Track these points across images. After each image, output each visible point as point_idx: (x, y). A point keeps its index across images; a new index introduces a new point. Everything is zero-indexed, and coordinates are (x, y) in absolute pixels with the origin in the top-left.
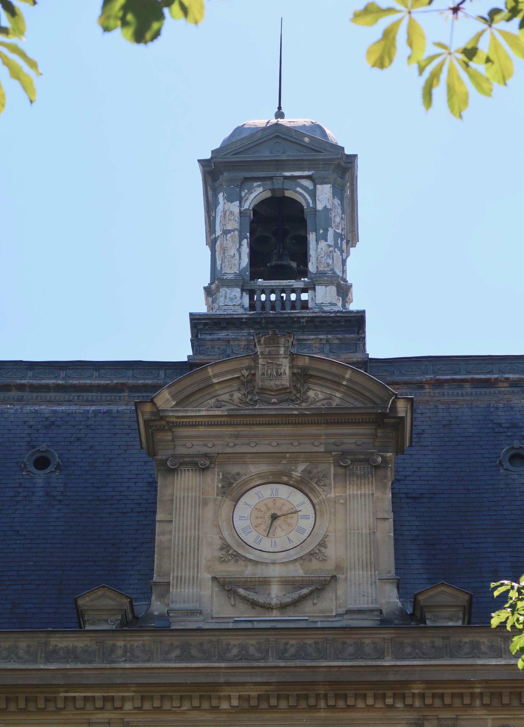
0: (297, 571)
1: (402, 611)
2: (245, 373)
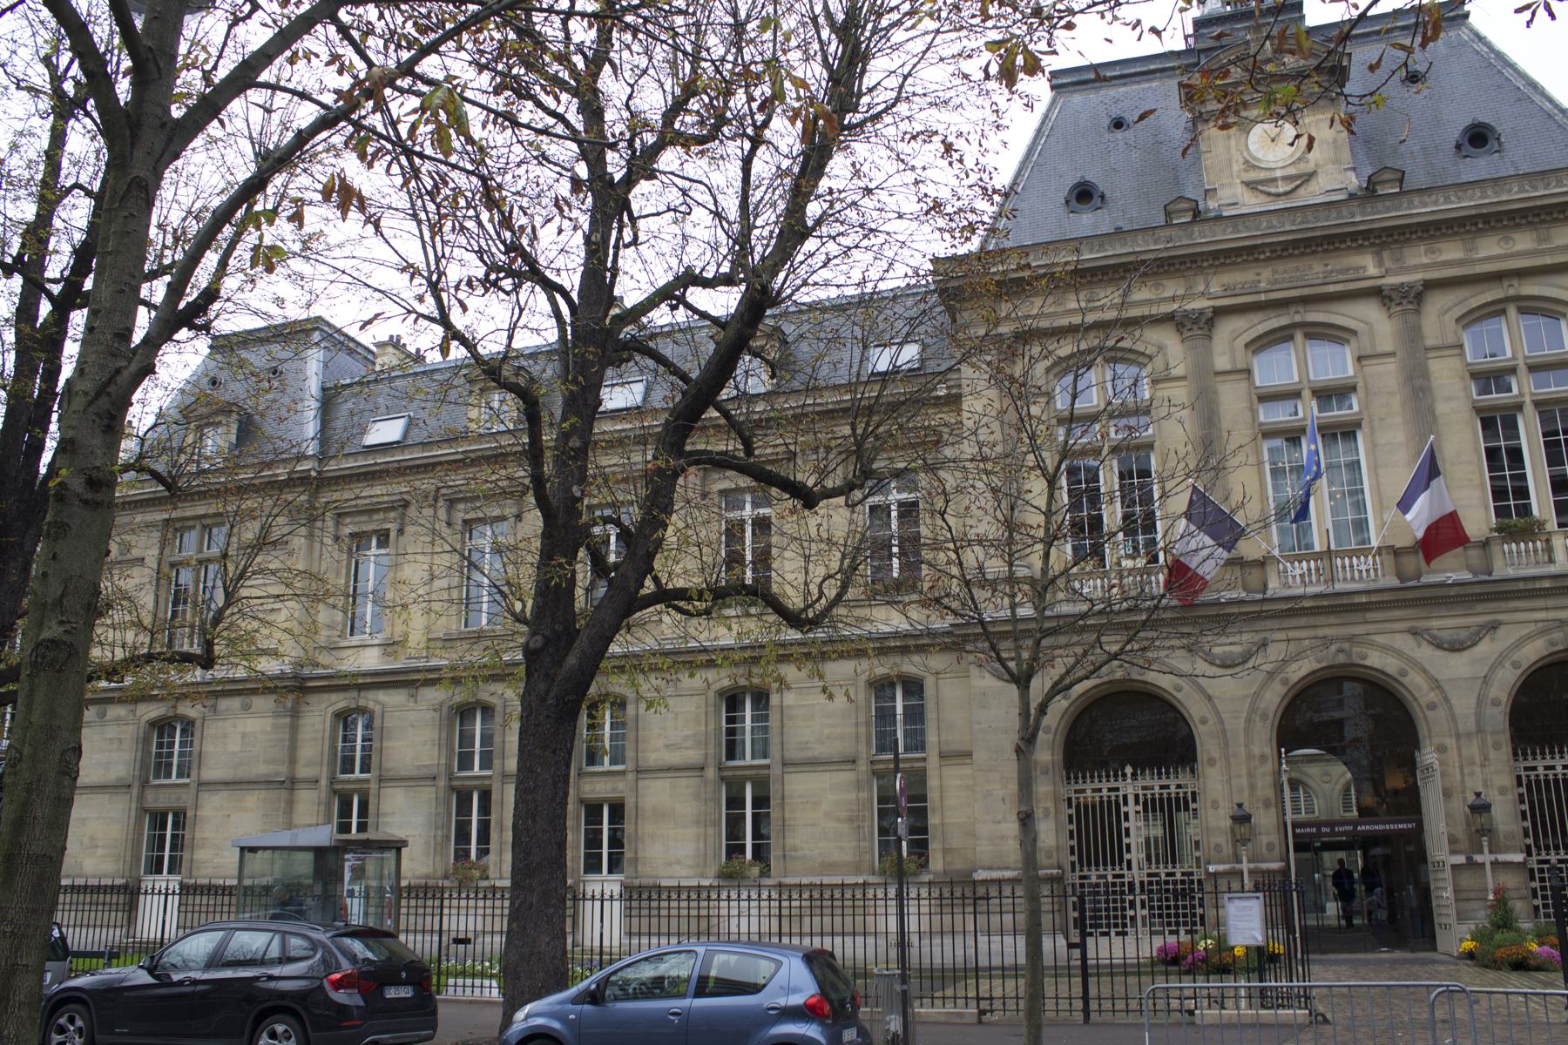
0: (1292, 171)
1: (1360, 188)
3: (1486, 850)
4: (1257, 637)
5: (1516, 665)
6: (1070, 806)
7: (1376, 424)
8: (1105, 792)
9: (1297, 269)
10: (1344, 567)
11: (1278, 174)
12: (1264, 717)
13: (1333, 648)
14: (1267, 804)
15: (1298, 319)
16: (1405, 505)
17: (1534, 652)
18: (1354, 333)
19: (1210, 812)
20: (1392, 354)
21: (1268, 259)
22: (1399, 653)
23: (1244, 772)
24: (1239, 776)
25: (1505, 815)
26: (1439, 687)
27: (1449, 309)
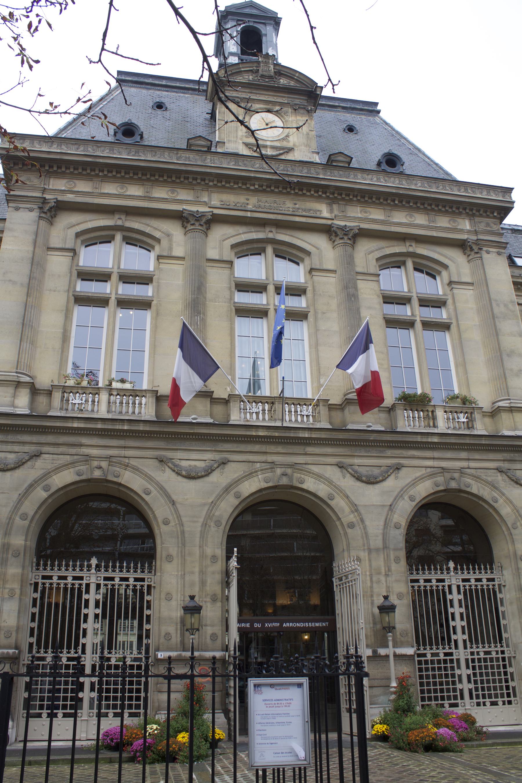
2: (255, 68)
3: (390, 644)
4: (217, 456)
5: (412, 498)
6: (36, 591)
7: (320, 315)
8: (70, 580)
9: (275, 202)
10: (290, 412)
11: (268, 143)
12: (218, 523)
13: (279, 471)
14: (214, 599)
15: (270, 238)
16: (345, 364)
17: (424, 490)
18: (308, 253)
19: (164, 603)
20: (334, 271)
21: (256, 191)
22: (329, 482)
23: (197, 570)
24: (193, 573)
25: (403, 619)
26: (357, 510)
27: (373, 252)
